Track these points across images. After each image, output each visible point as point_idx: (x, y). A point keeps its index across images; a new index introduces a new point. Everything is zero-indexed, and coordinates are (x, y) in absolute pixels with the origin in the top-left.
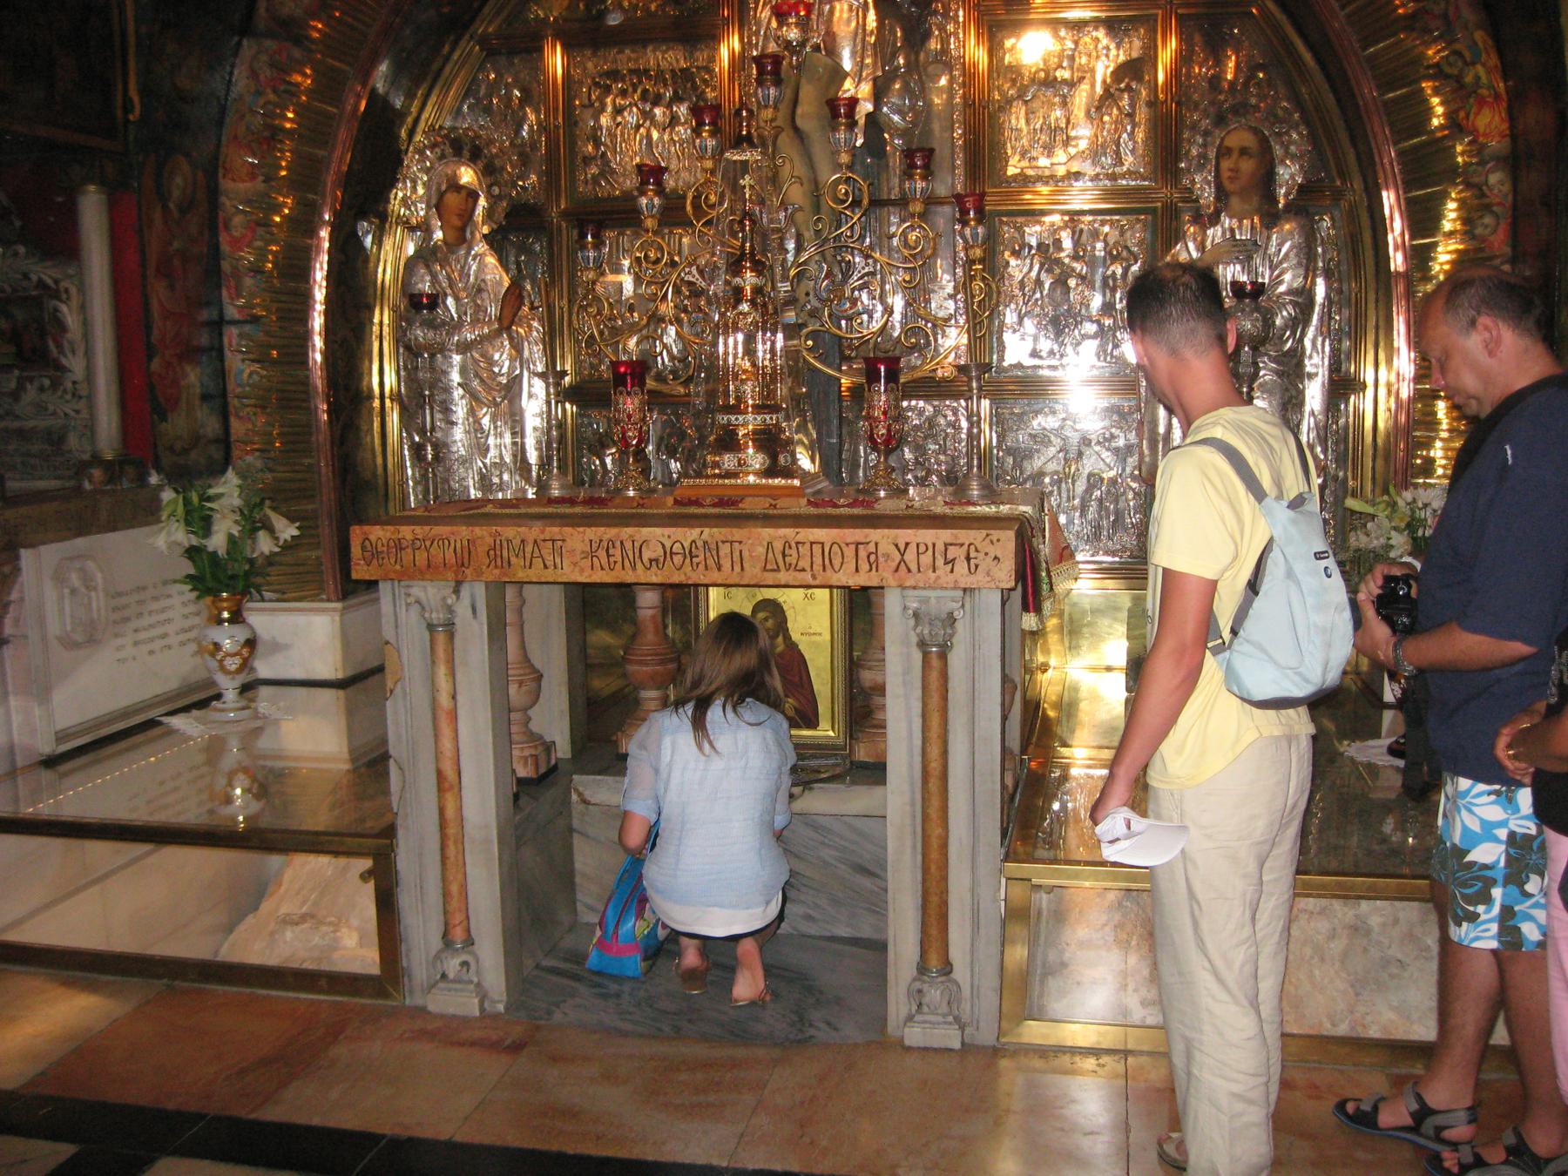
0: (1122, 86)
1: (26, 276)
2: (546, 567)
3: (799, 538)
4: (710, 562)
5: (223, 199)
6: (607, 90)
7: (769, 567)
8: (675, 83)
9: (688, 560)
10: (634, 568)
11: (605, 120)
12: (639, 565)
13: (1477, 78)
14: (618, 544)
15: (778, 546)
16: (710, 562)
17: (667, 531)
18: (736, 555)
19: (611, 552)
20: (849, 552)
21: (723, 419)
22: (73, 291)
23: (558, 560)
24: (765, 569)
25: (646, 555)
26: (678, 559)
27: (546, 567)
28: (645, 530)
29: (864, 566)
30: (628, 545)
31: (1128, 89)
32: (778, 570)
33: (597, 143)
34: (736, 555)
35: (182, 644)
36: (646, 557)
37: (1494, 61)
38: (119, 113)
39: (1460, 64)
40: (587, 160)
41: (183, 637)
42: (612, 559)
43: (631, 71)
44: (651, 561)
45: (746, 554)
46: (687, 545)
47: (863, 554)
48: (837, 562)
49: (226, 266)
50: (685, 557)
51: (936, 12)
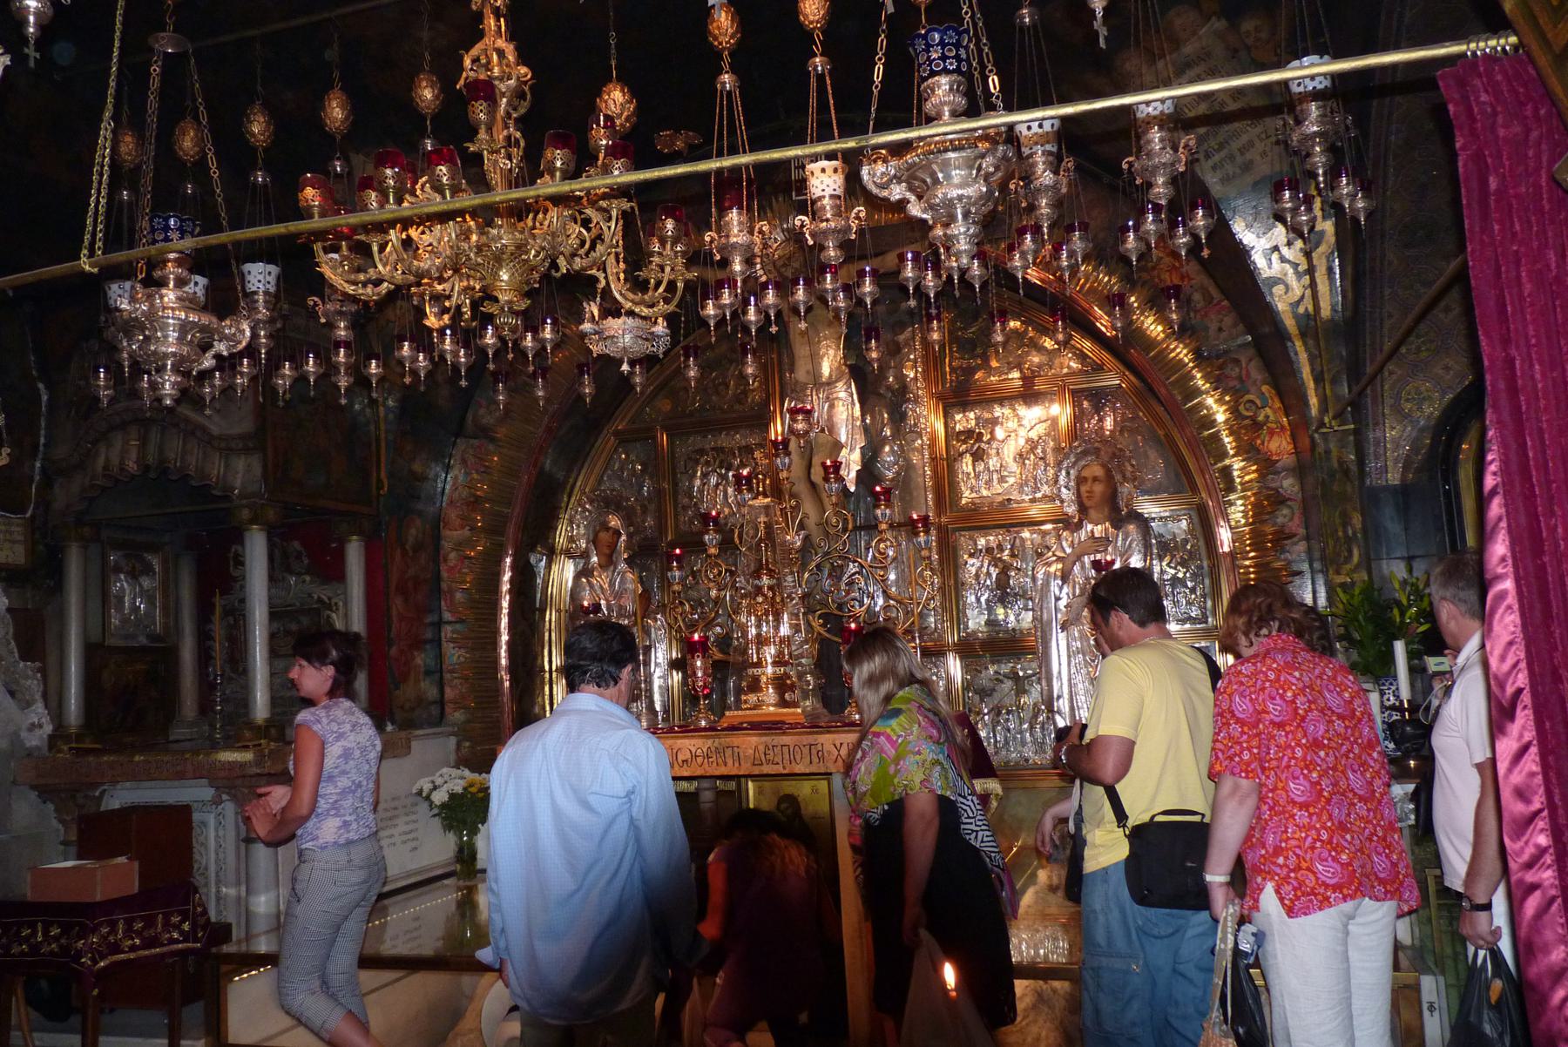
1: (310, 595)
3: (775, 743)
4: (720, 761)
5: (443, 542)
6: (697, 462)
8: (740, 455)
11: (698, 482)
13: (1267, 417)
15: (761, 748)
16: (720, 761)
17: (693, 741)
20: (805, 751)
21: (750, 671)
22: (341, 604)
25: (681, 757)
26: (700, 760)
28: (679, 741)
29: (815, 760)
33: (691, 497)
35: (404, 842)
37: (1278, 404)
38: (374, 489)
40: (685, 508)
41: (405, 838)
43: (713, 449)
45: (741, 755)
47: (814, 752)
48: (798, 757)
49: (444, 586)
51: (909, 400)
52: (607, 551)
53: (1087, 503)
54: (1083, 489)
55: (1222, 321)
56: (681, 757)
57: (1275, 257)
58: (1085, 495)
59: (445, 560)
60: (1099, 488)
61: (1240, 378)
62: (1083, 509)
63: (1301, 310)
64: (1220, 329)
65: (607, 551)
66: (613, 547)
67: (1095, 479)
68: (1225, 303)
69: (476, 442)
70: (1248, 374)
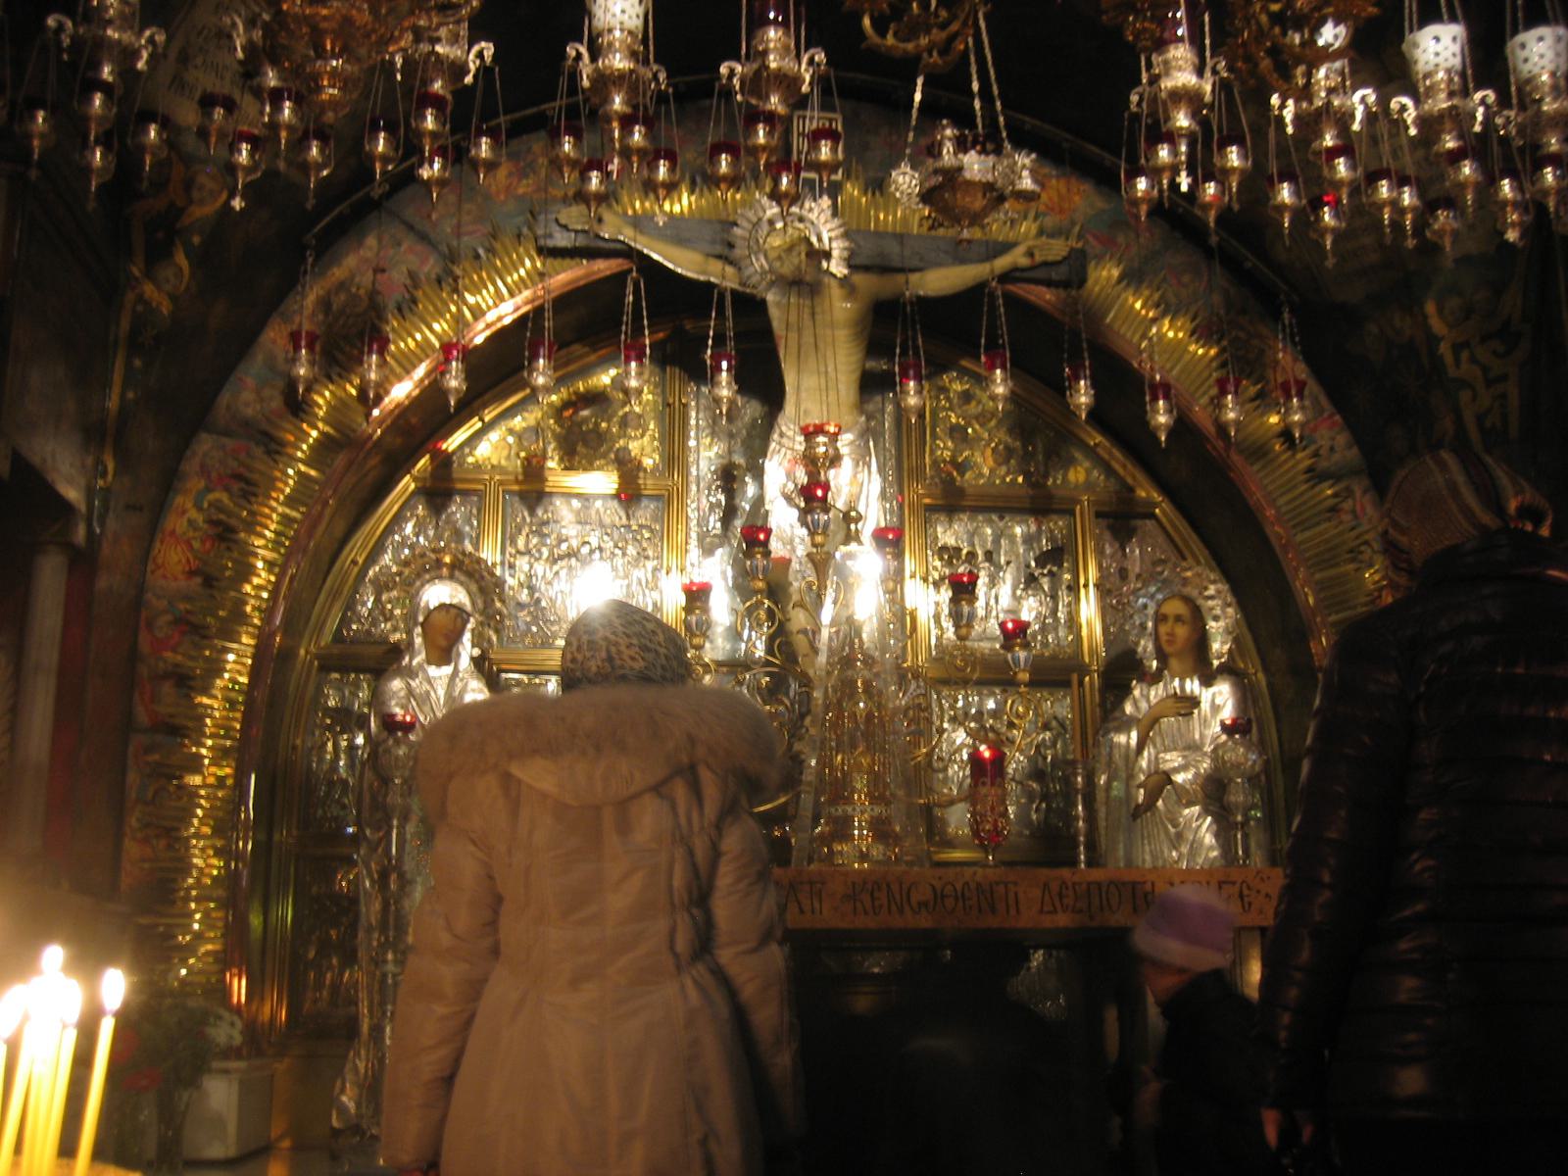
0: (1045, 571)
2: (802, 912)
5: (149, 596)
7: (1046, 909)
9: (961, 903)
10: (901, 911)
12: (907, 908)
14: (884, 886)
18: (1011, 896)
19: (876, 894)
23: (817, 905)
24: (1041, 911)
25: (915, 898)
26: (949, 903)
27: (802, 912)
30: (895, 887)
31: (1051, 574)
32: (1055, 911)
34: (1011, 896)
36: (914, 901)
39: (1369, 551)
42: (877, 903)
44: (919, 904)
46: (959, 887)
50: (957, 899)
52: (443, 643)
53: (1168, 649)
54: (1163, 629)
55: (1333, 439)
56: (915, 898)
57: (1465, 355)
58: (1164, 638)
59: (150, 626)
60: (1182, 632)
61: (1353, 512)
62: (1162, 656)
63: (1488, 424)
64: (1332, 449)
65: (443, 643)
66: (455, 637)
67: (1178, 618)
68: (1337, 418)
69: (229, 443)
70: (1363, 508)
